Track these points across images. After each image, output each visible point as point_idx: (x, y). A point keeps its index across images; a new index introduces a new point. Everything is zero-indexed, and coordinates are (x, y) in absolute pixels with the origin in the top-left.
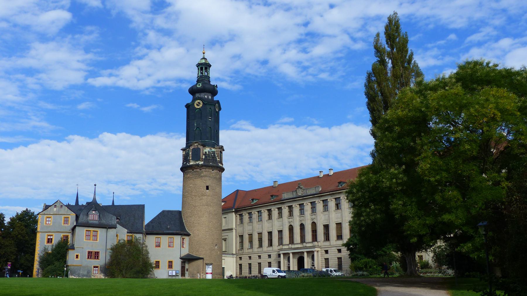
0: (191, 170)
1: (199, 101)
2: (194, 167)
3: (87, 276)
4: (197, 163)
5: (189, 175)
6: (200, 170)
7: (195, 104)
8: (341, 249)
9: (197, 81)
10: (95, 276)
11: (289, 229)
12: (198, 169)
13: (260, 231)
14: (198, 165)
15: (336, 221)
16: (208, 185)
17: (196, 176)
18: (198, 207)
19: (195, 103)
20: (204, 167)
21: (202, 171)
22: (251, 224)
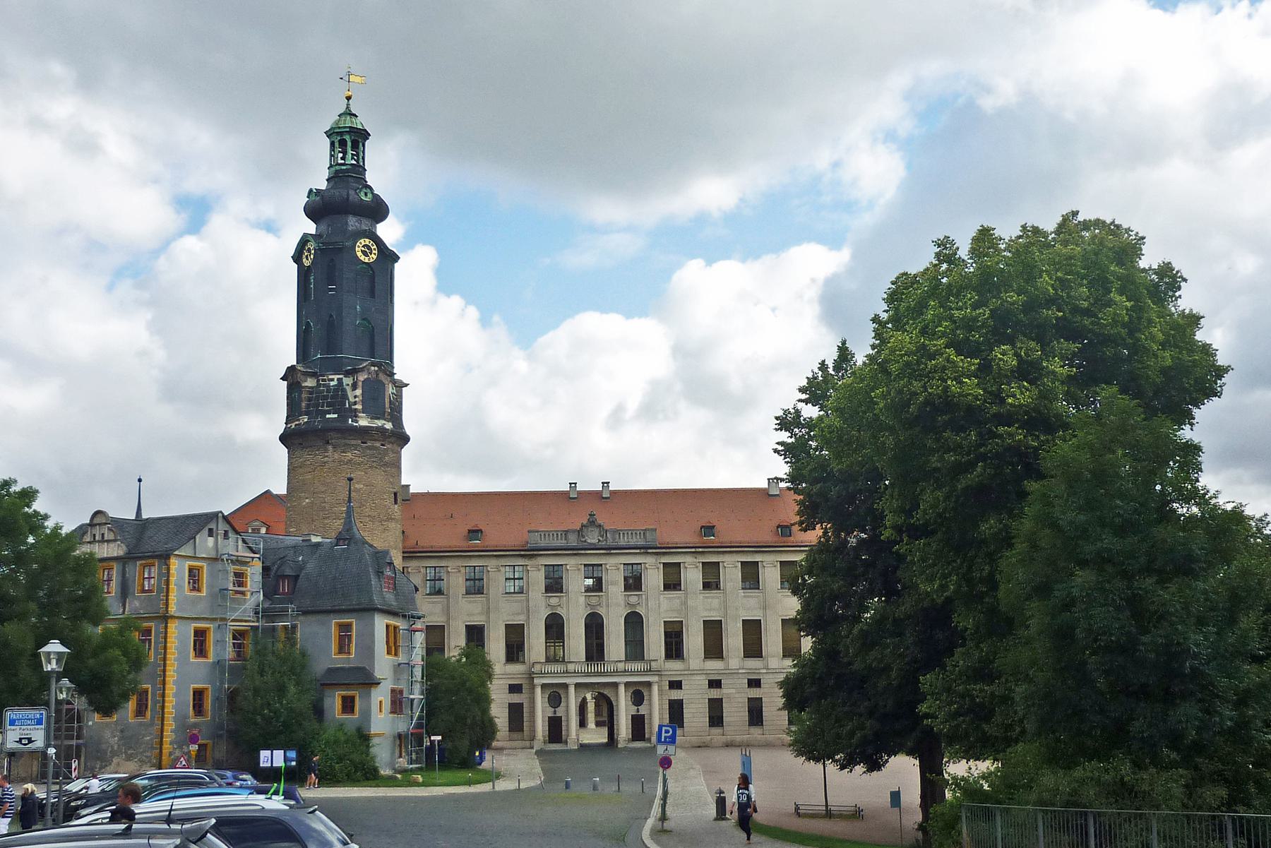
4: (379, 423)
6: (382, 445)
7: (357, 249)
8: (721, 680)
9: (327, 180)
12: (380, 441)
13: (481, 621)
14: (382, 430)
15: (706, 614)
19: (358, 244)
20: (392, 439)
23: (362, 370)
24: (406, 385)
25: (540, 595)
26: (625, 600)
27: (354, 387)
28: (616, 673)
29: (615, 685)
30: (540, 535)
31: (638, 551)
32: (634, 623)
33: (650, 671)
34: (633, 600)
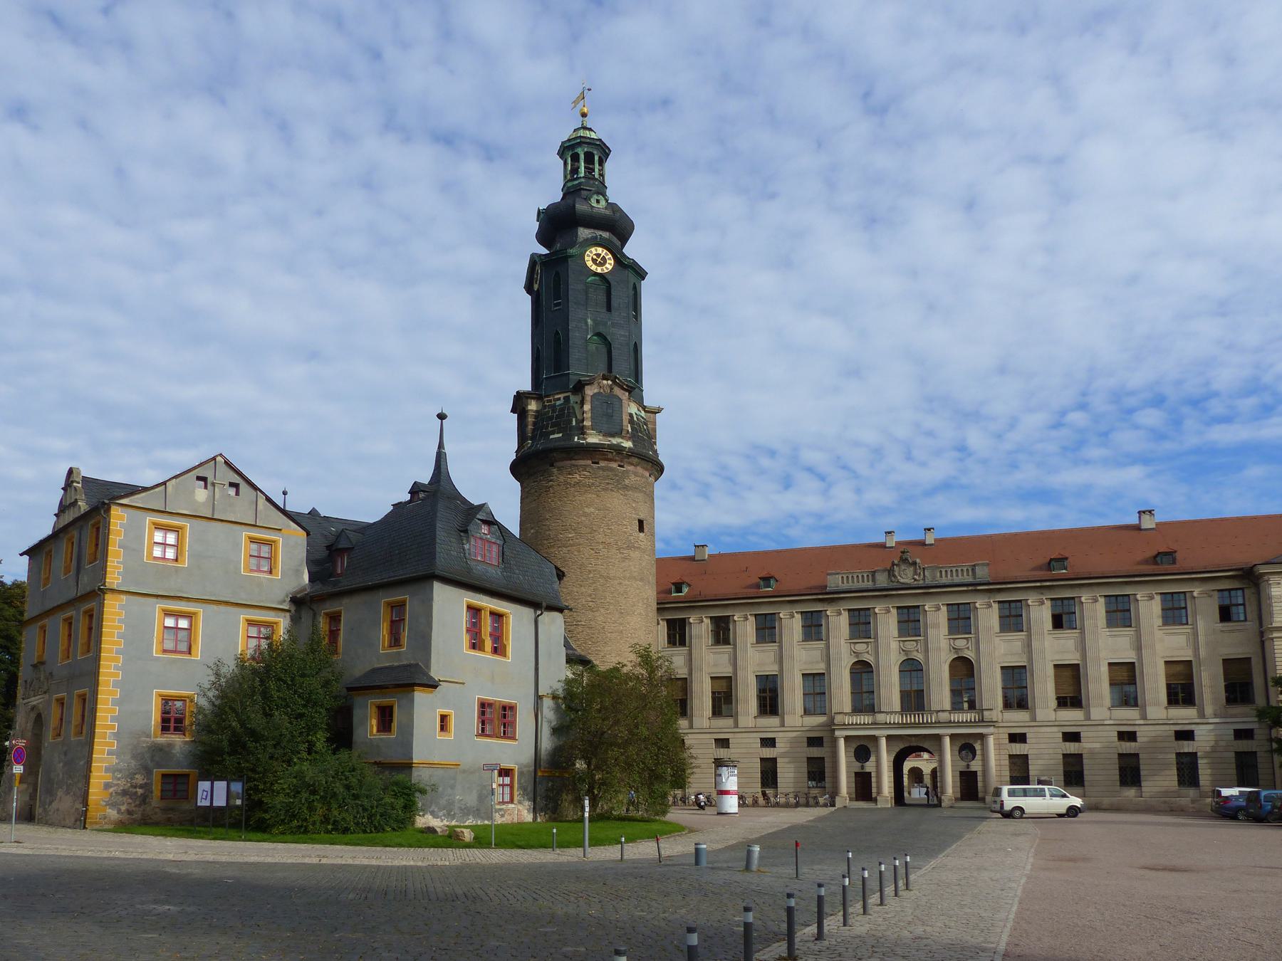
0: (589, 462)
1: (610, 256)
2: (603, 454)
3: (477, 813)
4: (615, 441)
5: (578, 477)
6: (619, 466)
10: (505, 811)
11: (851, 673)
12: (616, 461)
14: (619, 450)
16: (642, 517)
17: (608, 484)
18: (616, 582)
20: (635, 460)
21: (627, 471)
22: (680, 652)
23: (590, 383)
24: (659, 411)
25: (843, 642)
26: (950, 645)
27: (582, 403)
28: (938, 724)
29: (938, 738)
30: (842, 577)
31: (965, 589)
32: (964, 670)
33: (983, 721)
34: (961, 643)
